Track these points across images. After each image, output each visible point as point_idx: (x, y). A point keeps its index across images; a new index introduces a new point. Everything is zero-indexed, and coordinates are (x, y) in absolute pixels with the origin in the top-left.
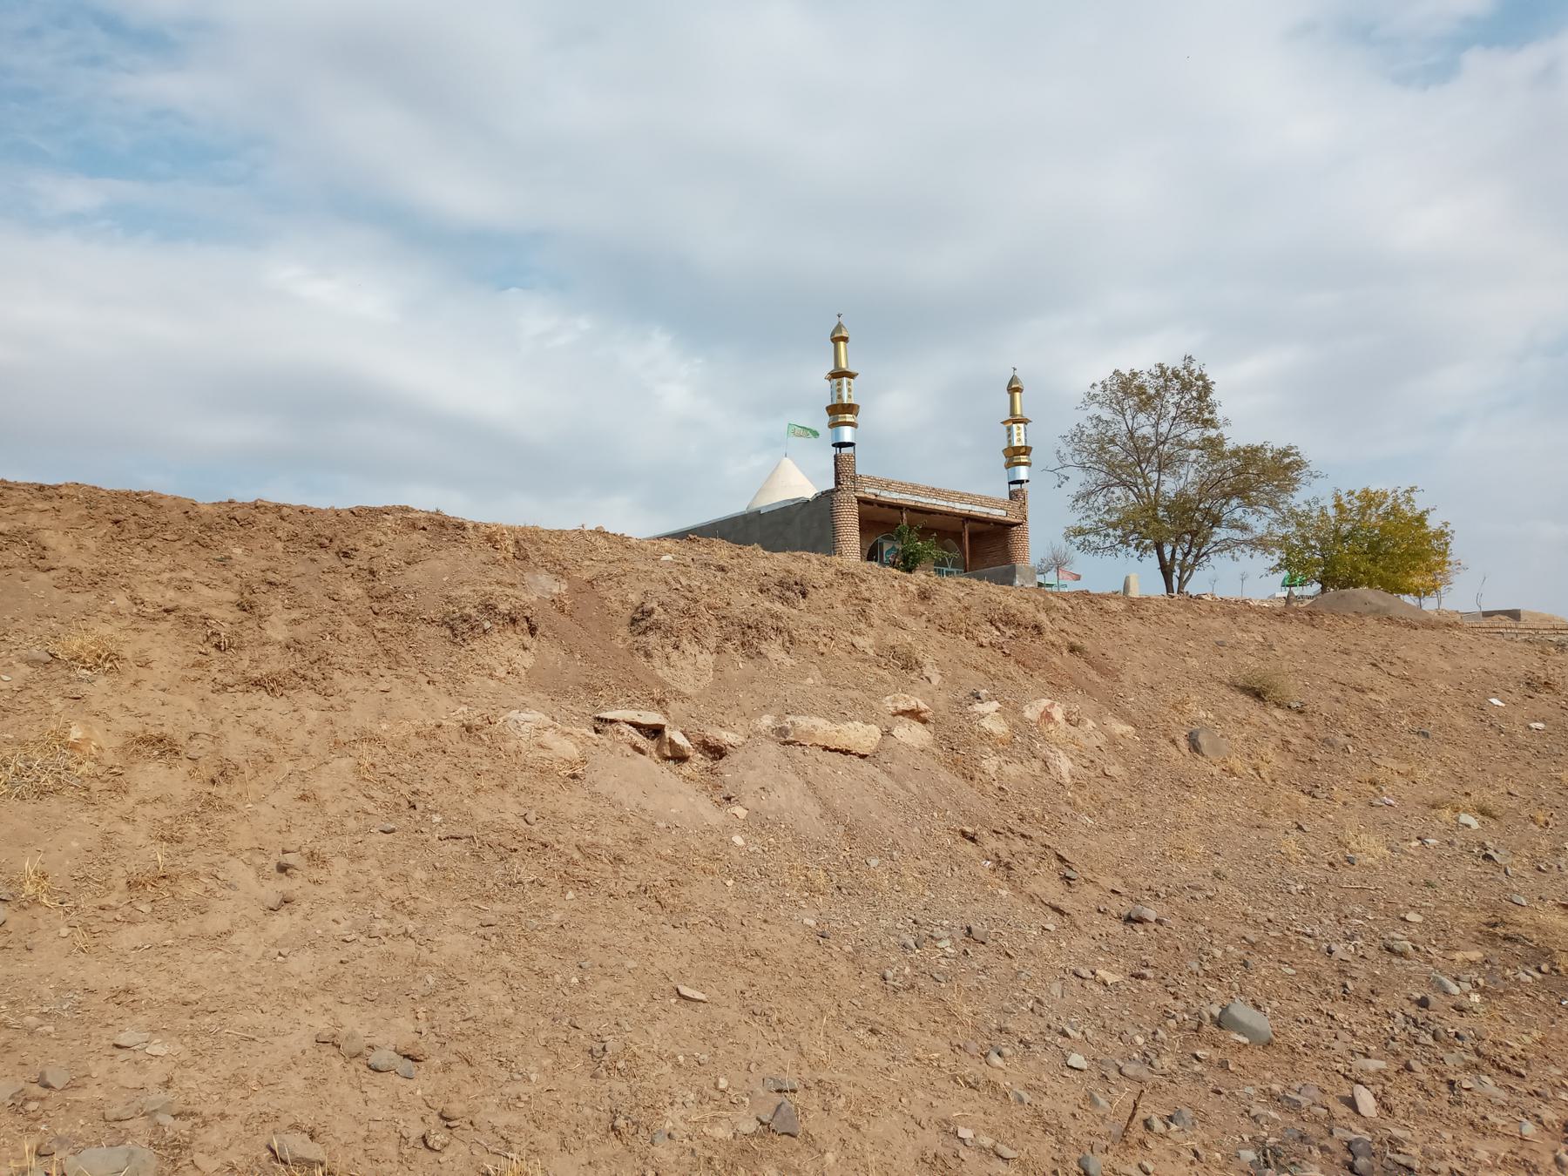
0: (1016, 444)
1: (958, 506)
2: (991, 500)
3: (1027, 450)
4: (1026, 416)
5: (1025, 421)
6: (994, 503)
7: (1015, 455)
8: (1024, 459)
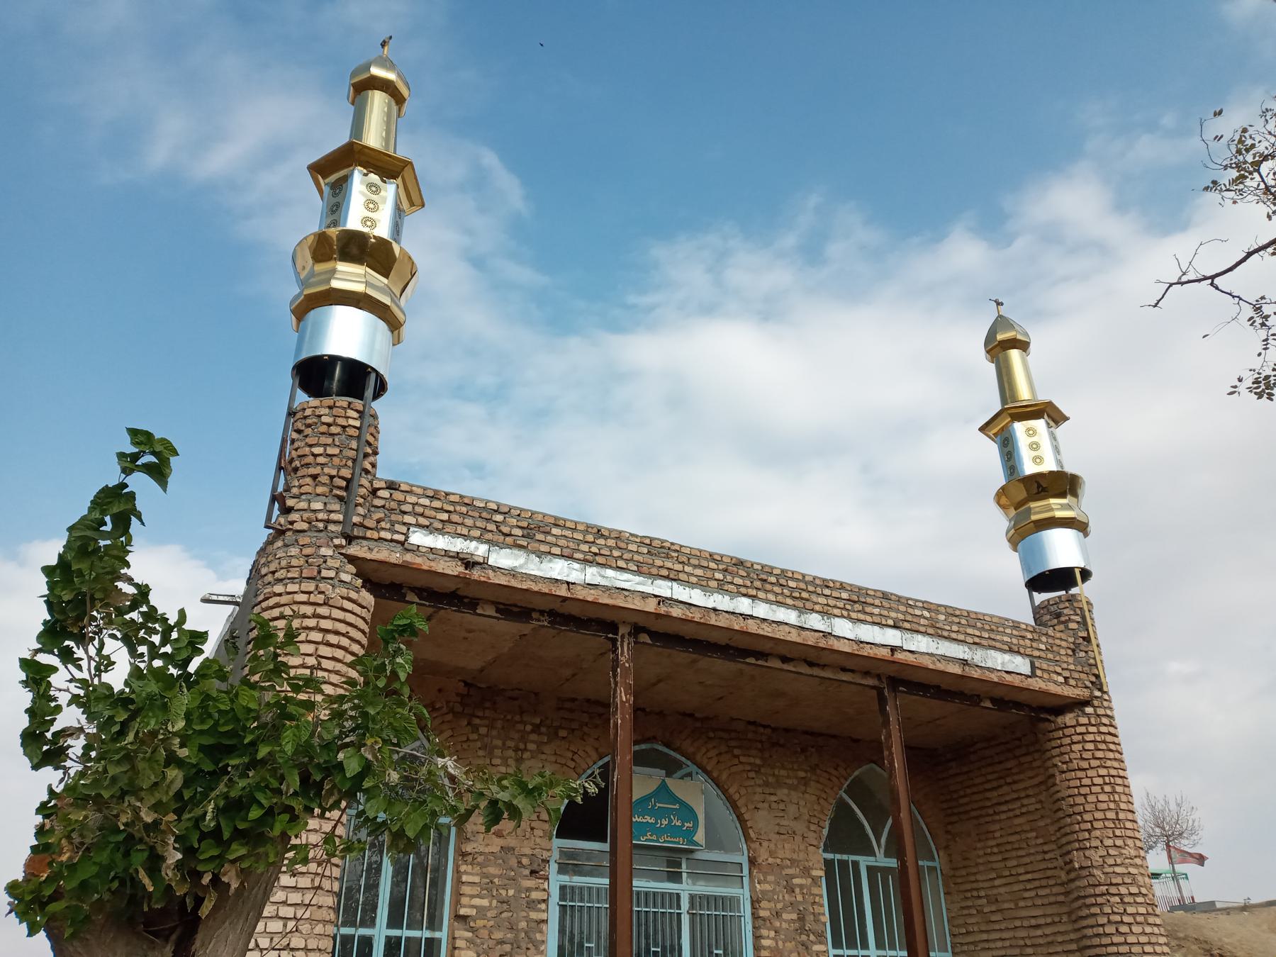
0: (1029, 468)
1: (843, 628)
2: (972, 619)
3: (1062, 484)
4: (1043, 397)
5: (1051, 414)
6: (982, 629)
7: (1035, 497)
8: (1057, 507)
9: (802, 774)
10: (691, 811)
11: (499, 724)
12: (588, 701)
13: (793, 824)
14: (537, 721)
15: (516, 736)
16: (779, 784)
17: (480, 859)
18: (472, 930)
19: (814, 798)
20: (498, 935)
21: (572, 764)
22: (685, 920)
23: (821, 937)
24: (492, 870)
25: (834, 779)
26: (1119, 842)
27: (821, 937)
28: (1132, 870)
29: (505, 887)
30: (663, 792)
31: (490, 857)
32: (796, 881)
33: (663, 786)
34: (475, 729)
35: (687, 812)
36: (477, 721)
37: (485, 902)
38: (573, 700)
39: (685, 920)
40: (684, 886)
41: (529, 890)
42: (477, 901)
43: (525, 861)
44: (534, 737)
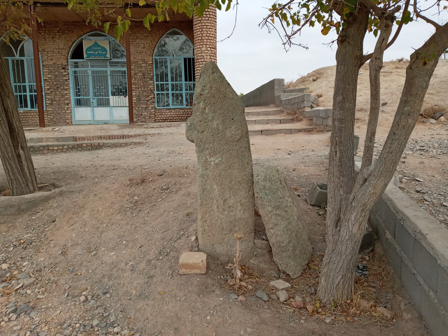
9: (146, 34)
10: (105, 48)
11: (47, 32)
12: (73, 22)
13: (141, 49)
14: (58, 29)
15: (53, 34)
16: (137, 38)
17: (48, 66)
18: (48, 82)
19: (150, 41)
20: (55, 83)
21: (70, 40)
22: (109, 77)
23: (152, 79)
24: (51, 68)
25: (158, 35)
26: (201, 46)
27: (152, 79)
28: (203, 54)
29: (55, 72)
30: (96, 44)
31: (50, 66)
32: (143, 65)
33: (96, 43)
34: (41, 33)
35: (105, 50)
36: (40, 31)
37: (50, 76)
38: (69, 22)
39: (109, 77)
40: (108, 68)
41: (62, 72)
42: (48, 76)
43: (60, 66)
44: (57, 34)
